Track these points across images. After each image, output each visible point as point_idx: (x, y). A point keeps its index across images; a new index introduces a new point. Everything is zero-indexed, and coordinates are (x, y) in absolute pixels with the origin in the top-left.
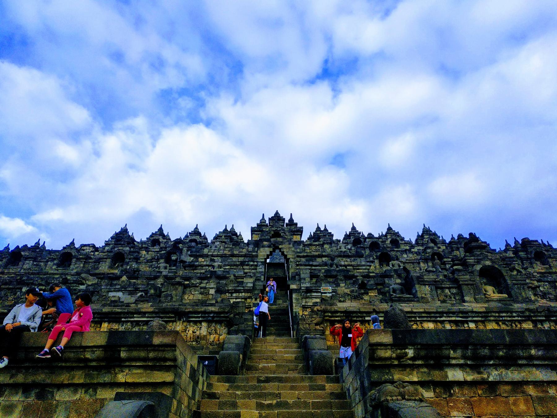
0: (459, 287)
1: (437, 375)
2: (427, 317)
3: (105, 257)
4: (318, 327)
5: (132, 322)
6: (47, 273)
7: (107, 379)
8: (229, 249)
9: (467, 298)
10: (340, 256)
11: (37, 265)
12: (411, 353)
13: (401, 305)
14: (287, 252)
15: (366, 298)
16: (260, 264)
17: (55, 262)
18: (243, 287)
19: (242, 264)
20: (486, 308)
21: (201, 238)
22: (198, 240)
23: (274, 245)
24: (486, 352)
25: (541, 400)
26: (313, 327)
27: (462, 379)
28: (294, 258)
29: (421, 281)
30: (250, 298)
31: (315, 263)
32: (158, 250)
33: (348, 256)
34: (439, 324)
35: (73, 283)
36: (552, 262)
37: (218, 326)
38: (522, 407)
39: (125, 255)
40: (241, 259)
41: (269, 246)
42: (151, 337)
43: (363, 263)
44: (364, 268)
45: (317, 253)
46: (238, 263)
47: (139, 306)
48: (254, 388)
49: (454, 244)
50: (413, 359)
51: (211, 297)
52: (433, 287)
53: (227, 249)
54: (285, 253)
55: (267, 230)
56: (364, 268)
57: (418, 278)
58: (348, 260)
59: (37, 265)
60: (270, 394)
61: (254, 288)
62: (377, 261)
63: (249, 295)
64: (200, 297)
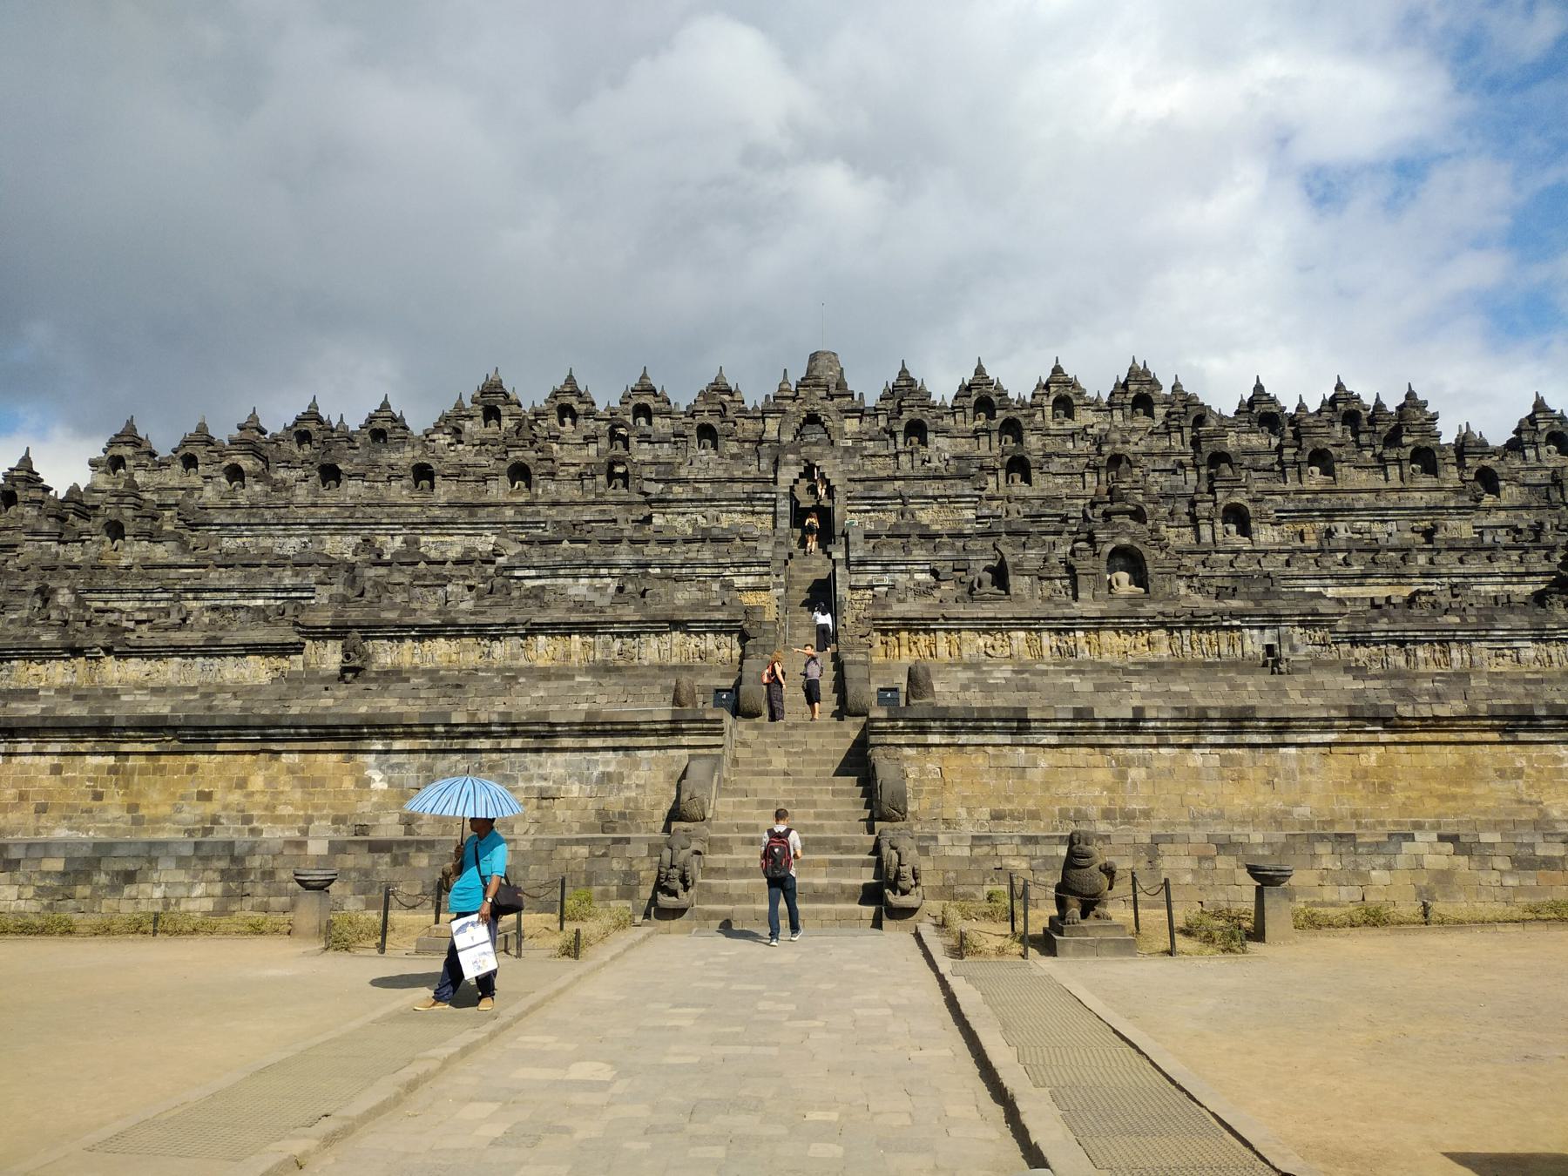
1: (920, 739)
2: (1017, 624)
3: (494, 472)
4: (863, 640)
5: (611, 633)
6: (396, 505)
7: (674, 743)
8: (724, 467)
10: (927, 478)
11: (371, 488)
13: (983, 606)
14: (830, 474)
15: (937, 594)
16: (781, 497)
17: (404, 482)
18: (757, 557)
20: (1101, 611)
21: (657, 399)
22: (652, 407)
23: (806, 461)
24: (959, 724)
25: (995, 757)
27: (938, 742)
28: (844, 486)
29: (1020, 570)
30: (768, 574)
31: (879, 494)
32: (582, 441)
33: (942, 478)
34: (1033, 633)
35: (446, 523)
36: (1341, 470)
38: (980, 761)
39: (531, 468)
41: (798, 464)
42: (704, 714)
43: (967, 492)
44: (968, 499)
45: (883, 474)
47: (618, 612)
48: (782, 735)
49: (1175, 420)
50: (903, 728)
51: (714, 595)
52: (1035, 578)
53: (721, 467)
54: (827, 477)
55: (794, 409)
56: (968, 499)
57: (1015, 565)
58: (941, 486)
59: (371, 488)
60: (797, 742)
62: (1002, 473)
63: (766, 569)
64: (699, 595)
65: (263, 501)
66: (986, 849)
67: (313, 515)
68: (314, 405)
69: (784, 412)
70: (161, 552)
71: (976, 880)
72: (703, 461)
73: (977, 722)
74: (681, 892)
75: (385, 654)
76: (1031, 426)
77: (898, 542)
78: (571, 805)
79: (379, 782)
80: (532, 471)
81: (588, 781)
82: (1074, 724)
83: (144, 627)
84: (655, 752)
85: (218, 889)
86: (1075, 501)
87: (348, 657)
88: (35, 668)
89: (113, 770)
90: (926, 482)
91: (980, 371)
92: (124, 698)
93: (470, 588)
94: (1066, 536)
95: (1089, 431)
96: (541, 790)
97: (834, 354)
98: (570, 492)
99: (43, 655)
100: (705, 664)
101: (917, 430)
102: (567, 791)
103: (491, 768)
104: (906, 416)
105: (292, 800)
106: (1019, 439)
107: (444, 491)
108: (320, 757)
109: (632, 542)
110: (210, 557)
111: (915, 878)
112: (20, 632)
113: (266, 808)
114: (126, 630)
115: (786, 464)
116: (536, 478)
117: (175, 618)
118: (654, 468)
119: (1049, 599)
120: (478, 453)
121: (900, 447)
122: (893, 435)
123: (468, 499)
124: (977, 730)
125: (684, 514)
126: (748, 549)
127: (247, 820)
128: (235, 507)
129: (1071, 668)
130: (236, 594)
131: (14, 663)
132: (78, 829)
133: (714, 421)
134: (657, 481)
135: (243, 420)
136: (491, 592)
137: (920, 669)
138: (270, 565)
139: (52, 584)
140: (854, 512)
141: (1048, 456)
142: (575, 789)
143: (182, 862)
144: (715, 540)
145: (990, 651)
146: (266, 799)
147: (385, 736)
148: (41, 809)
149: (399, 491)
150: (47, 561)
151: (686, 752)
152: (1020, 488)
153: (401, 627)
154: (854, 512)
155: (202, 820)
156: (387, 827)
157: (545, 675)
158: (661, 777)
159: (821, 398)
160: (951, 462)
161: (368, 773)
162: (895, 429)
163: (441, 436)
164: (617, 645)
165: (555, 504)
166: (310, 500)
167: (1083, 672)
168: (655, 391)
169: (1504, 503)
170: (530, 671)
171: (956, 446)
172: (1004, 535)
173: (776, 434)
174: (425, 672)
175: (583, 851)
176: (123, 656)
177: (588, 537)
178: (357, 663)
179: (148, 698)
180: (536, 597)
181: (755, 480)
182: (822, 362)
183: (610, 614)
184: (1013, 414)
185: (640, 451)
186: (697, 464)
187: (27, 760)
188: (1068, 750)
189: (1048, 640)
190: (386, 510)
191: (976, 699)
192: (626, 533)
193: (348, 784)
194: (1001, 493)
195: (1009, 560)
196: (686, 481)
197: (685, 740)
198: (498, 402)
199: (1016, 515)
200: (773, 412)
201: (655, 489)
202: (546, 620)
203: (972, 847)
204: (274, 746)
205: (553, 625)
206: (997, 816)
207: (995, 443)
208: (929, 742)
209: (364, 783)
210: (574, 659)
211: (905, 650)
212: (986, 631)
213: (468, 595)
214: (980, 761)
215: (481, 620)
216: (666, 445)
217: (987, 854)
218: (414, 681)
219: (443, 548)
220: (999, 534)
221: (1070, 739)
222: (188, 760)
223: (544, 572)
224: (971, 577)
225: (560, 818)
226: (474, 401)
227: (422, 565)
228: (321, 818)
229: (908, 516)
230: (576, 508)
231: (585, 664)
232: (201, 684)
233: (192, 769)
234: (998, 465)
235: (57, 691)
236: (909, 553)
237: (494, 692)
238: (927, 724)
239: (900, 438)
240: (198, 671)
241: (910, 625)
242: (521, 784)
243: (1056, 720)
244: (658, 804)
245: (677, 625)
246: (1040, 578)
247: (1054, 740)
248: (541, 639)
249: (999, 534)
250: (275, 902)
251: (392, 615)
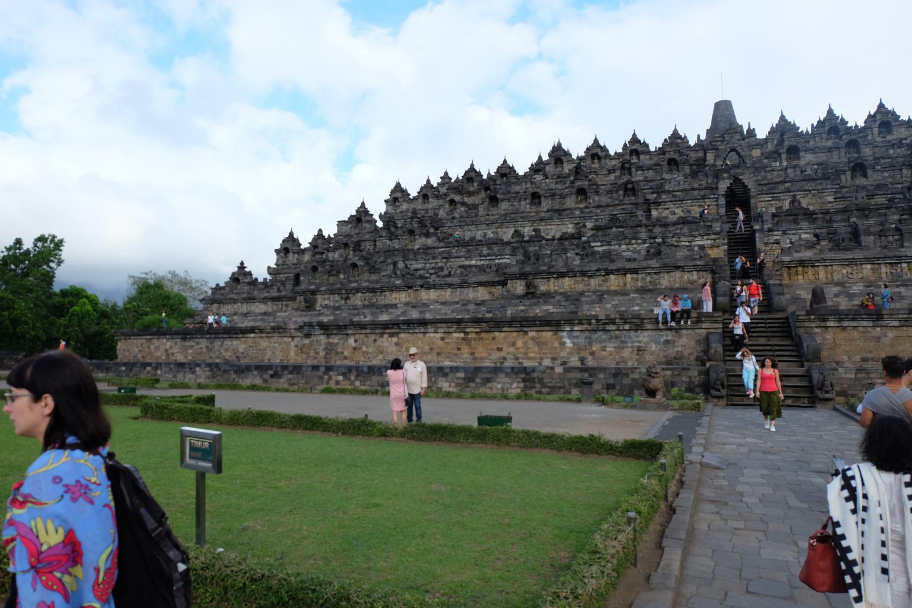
0: (901, 235)
1: (823, 324)
4: (778, 273)
6: (524, 212)
7: (698, 327)
9: (906, 244)
10: (804, 180)
11: (512, 205)
12: (813, 317)
15: (818, 247)
17: (528, 201)
19: (704, 198)
23: (734, 177)
24: (844, 317)
26: (774, 272)
30: (718, 239)
31: (776, 191)
33: (814, 180)
37: (704, 273)
38: (855, 334)
40: (702, 193)
41: (729, 178)
43: (829, 187)
46: (699, 197)
52: (877, 237)
54: (746, 184)
58: (813, 184)
59: (512, 205)
61: (722, 231)
62: (849, 174)
63: (718, 236)
64: (688, 253)
65: (465, 215)
66: (863, 375)
67: (488, 220)
68: (472, 165)
69: (717, 149)
70: (430, 242)
71: (858, 388)
72: (676, 180)
73: (855, 315)
74: (721, 390)
75: (543, 286)
76: (866, 143)
77: (791, 218)
78: (652, 353)
79: (569, 343)
80: (587, 190)
81: (659, 343)
82: (909, 316)
83: (434, 276)
84: (689, 331)
85: (522, 385)
86: (896, 186)
87: (529, 288)
88: (395, 295)
89: (463, 339)
90: (804, 183)
91: (830, 112)
92: (431, 307)
93: (577, 254)
94: (893, 210)
95: (904, 142)
96: (638, 347)
97: (730, 102)
98: (605, 200)
99: (397, 289)
100: (692, 287)
101: (793, 151)
102: (651, 348)
103: (616, 338)
104: (786, 144)
105: (534, 349)
106: (858, 151)
107: (546, 204)
108: (544, 333)
109: (646, 226)
110: (451, 243)
111: (832, 386)
112: (387, 280)
113: (524, 354)
114: (427, 277)
115: (723, 179)
116: (589, 194)
117: (446, 272)
118: (645, 183)
119: (885, 247)
120: (557, 183)
121: (785, 164)
122: (779, 154)
123: (557, 207)
124: (853, 320)
125: (668, 209)
126: (708, 226)
127: (517, 359)
128: (453, 218)
129: (899, 283)
130: (463, 259)
131: (387, 293)
132: (453, 362)
133: (676, 156)
134: (652, 193)
135: (442, 175)
136: (586, 256)
137: (819, 290)
138: (476, 245)
139: (396, 260)
140: (762, 201)
141: (878, 159)
142: (653, 347)
143: (507, 375)
144: (690, 223)
145: (850, 276)
146: (524, 350)
147: (570, 324)
148: (439, 354)
149: (525, 206)
150: (386, 248)
151: (703, 330)
152: (861, 181)
153: (549, 273)
154: (762, 201)
155: (500, 358)
156: (574, 361)
157: (616, 293)
158: (693, 342)
159: (738, 140)
160: (819, 171)
161: (564, 340)
162: (781, 151)
163: (537, 176)
164: (649, 279)
165: (599, 207)
166: (485, 213)
167: (907, 286)
168: (640, 141)
170: (608, 292)
171: (818, 158)
172: (855, 212)
173: (712, 161)
174: (561, 294)
175: (669, 373)
176: (429, 288)
177: (624, 224)
178: (533, 290)
179: (440, 307)
180: (607, 257)
181: (705, 189)
183: (644, 264)
184: (854, 137)
185: (637, 175)
186: (673, 182)
187: (432, 335)
188: (905, 328)
189: (884, 269)
190: (520, 215)
191: (844, 304)
192: (643, 222)
193: (556, 344)
194: (848, 184)
195: (861, 227)
196: (669, 192)
197: (704, 326)
198: (561, 155)
199: (861, 200)
200: (711, 150)
201: (652, 197)
202: (615, 268)
203: (856, 374)
204: (526, 329)
205: (618, 270)
206: (864, 360)
207: (843, 154)
208: (828, 325)
209: (563, 344)
210: (628, 286)
211: (800, 277)
212: (847, 265)
213: (578, 258)
214: (855, 334)
215: (585, 269)
216: (651, 171)
217: (864, 378)
218: (558, 298)
219: (547, 232)
220: (852, 211)
221: (906, 324)
222: (492, 335)
223: (605, 243)
224: (837, 237)
225: (648, 359)
226: (550, 155)
227: (544, 242)
228: (548, 358)
229: (796, 204)
230: (610, 208)
231: (634, 288)
232: (460, 300)
233: (494, 338)
234: (846, 169)
235: (404, 304)
236: (798, 224)
237: (593, 302)
238: (826, 317)
239: (784, 156)
240: (459, 295)
241: (802, 263)
242: (630, 345)
243: (898, 314)
244: (691, 354)
245: (677, 268)
246: (880, 236)
247: (897, 323)
248: (612, 277)
249: (852, 211)
250: (545, 390)
251: (545, 268)
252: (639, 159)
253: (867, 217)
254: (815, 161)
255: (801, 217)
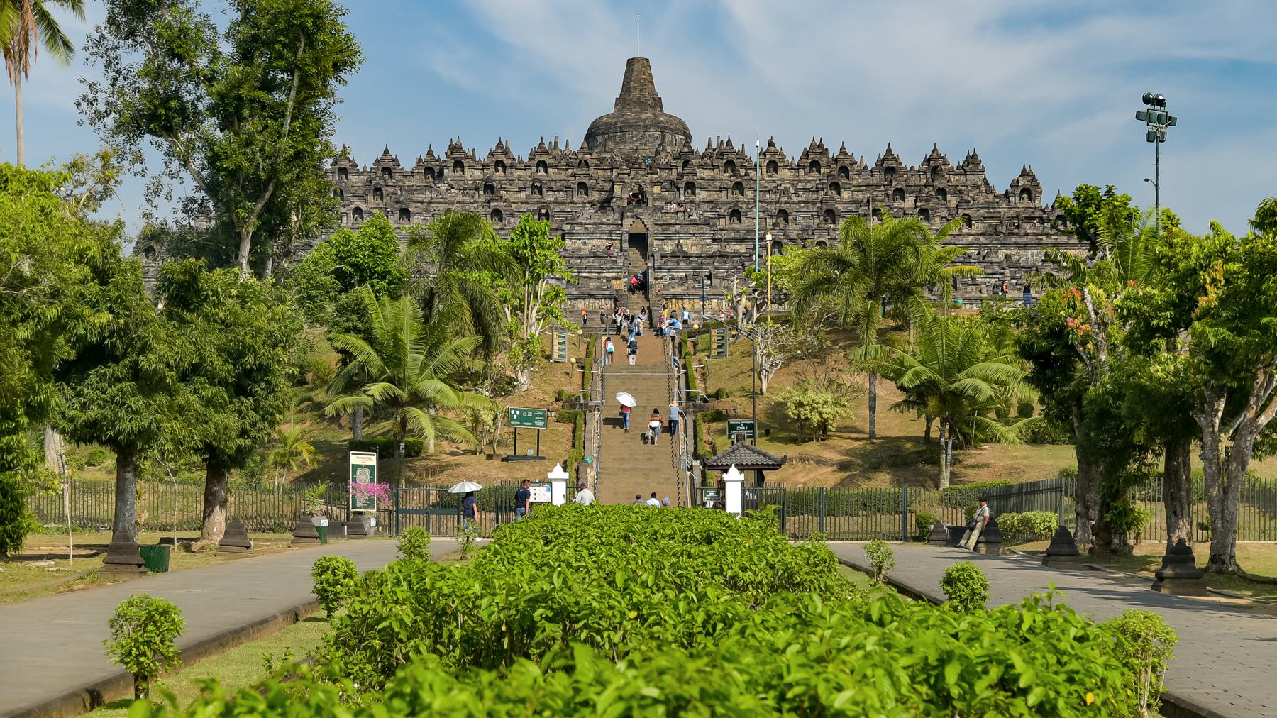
77: (675, 259)
104: (685, 179)
133: (586, 180)
152: (736, 225)
169: (973, 232)
182: (637, 67)
236: (679, 264)
241: (676, 297)
252: (546, 172)
253: (725, 262)
254: (708, 199)
255: (681, 259)
